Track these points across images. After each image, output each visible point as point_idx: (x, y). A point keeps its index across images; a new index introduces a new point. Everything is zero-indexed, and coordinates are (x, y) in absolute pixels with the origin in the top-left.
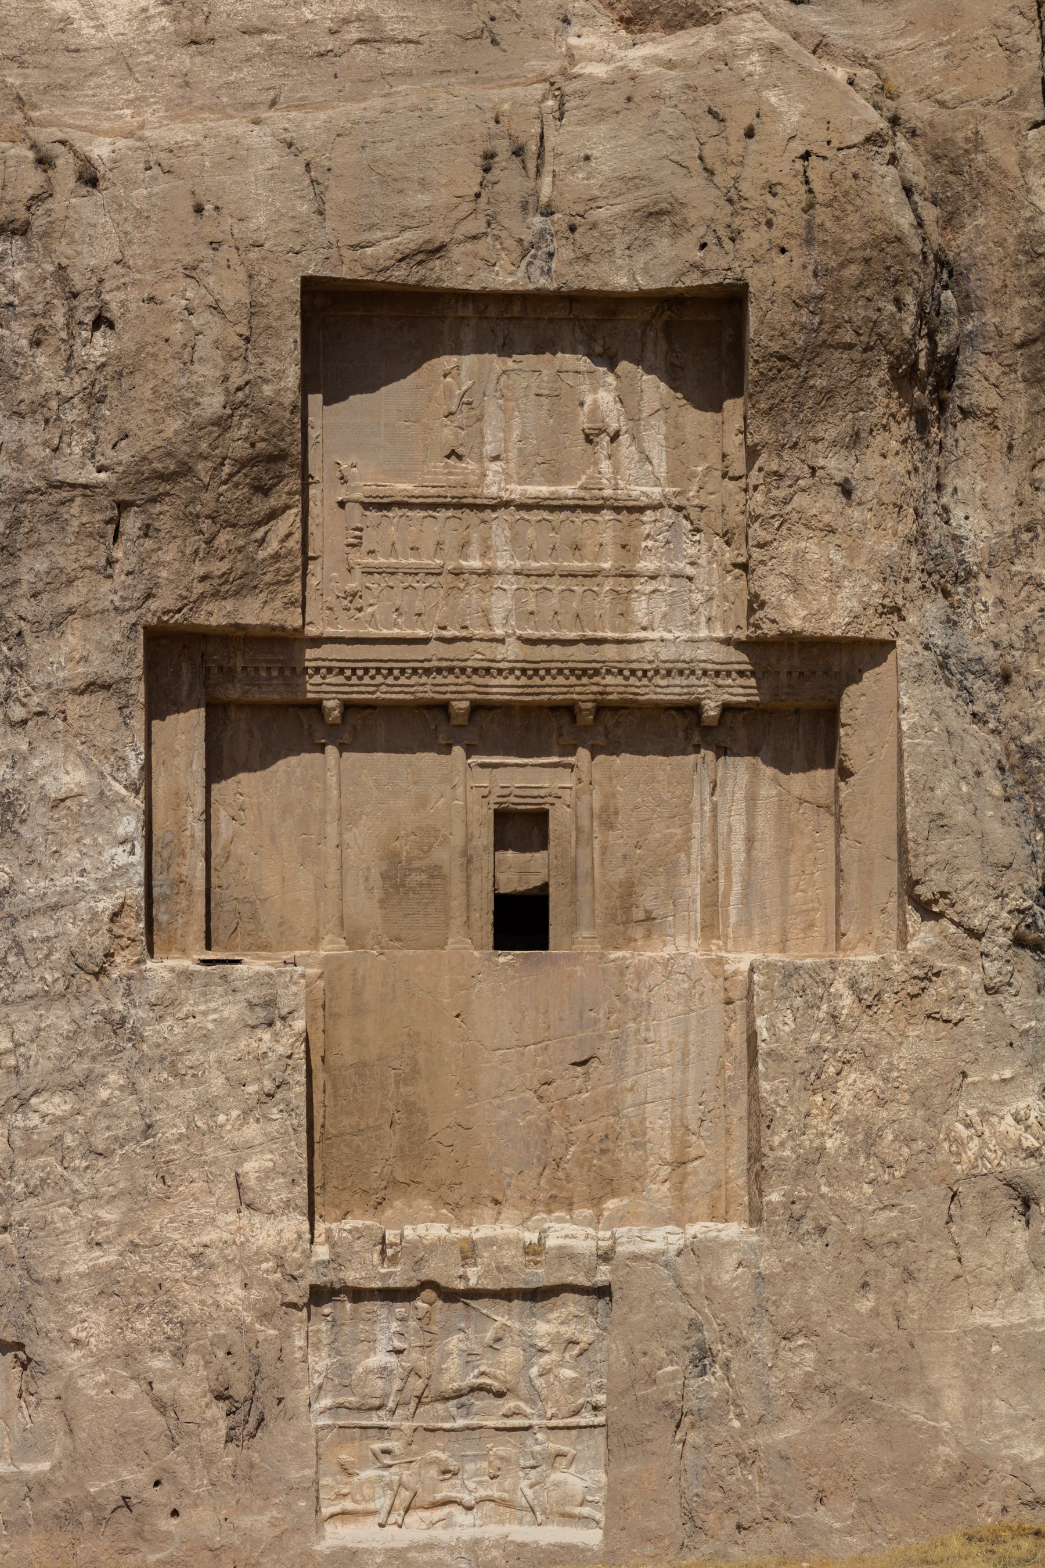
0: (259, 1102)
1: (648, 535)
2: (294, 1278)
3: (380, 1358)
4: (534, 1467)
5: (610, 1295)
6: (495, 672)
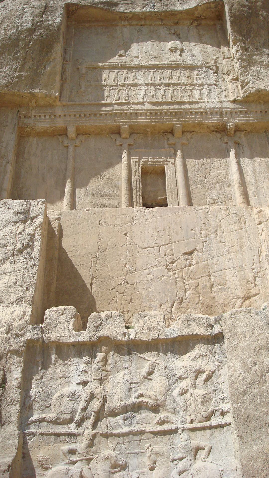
0: (13, 255)
1: (197, 75)
2: (17, 336)
3: (72, 387)
4: (181, 459)
6: (139, 115)
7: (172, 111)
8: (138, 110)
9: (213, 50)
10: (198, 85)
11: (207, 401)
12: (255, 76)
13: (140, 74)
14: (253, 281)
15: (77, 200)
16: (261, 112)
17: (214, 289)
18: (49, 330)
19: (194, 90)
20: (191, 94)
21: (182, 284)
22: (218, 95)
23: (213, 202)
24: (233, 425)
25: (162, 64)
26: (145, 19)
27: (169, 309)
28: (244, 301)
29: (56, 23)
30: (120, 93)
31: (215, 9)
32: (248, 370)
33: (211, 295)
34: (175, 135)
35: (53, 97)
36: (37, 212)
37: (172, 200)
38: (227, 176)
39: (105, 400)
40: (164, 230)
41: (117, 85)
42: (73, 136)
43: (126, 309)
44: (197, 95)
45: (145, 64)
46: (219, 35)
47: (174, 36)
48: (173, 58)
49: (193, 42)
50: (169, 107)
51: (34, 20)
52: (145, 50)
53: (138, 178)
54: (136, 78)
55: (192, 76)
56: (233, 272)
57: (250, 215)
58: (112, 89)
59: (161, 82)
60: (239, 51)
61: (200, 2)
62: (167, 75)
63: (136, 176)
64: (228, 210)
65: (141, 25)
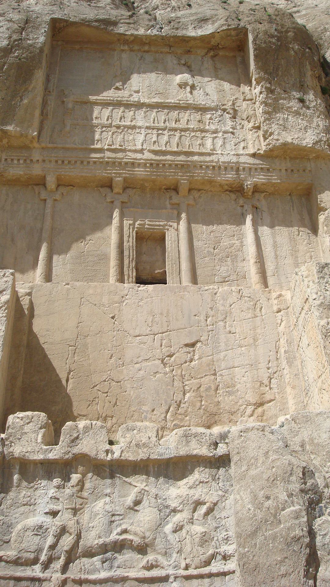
1: (211, 119)
5: (230, 461)
6: (136, 165)
7: (178, 162)
8: (136, 159)
9: (231, 89)
10: (210, 131)
11: (206, 541)
12: (281, 125)
13: (141, 113)
14: (268, 384)
15: (54, 269)
16: (286, 170)
17: (220, 391)
18: (11, 442)
19: (206, 138)
20: (202, 142)
21: (181, 385)
22: (235, 145)
23: (222, 280)
24: (238, 573)
25: (167, 103)
26: (149, 44)
27: (163, 415)
28: (256, 408)
29: (38, 43)
30: (114, 136)
31: (236, 37)
32: (259, 506)
33: (216, 400)
34: (180, 193)
35: (30, 137)
36: (3, 286)
37: (173, 275)
38: (241, 247)
39: (79, 536)
40: (162, 314)
41: (110, 126)
42: (52, 187)
43: (110, 414)
44: (209, 144)
45: (147, 101)
46: (239, 71)
47: (184, 68)
48: (182, 95)
49: (207, 77)
50: (174, 157)
51: (10, 37)
52: (147, 83)
53: (131, 244)
54: (135, 119)
55: (204, 120)
56: (244, 370)
57: (267, 299)
58: (104, 131)
59: (165, 125)
60: (263, 92)
61: (218, 28)
62: (173, 117)
63: (130, 243)
64: (241, 292)
65: (144, 51)
